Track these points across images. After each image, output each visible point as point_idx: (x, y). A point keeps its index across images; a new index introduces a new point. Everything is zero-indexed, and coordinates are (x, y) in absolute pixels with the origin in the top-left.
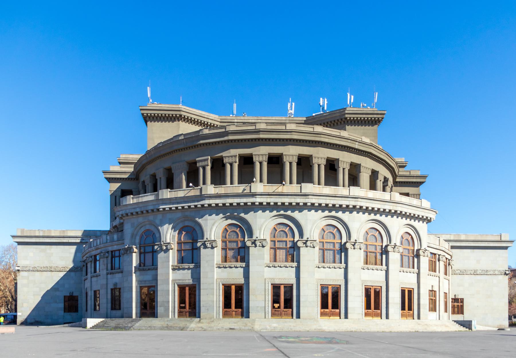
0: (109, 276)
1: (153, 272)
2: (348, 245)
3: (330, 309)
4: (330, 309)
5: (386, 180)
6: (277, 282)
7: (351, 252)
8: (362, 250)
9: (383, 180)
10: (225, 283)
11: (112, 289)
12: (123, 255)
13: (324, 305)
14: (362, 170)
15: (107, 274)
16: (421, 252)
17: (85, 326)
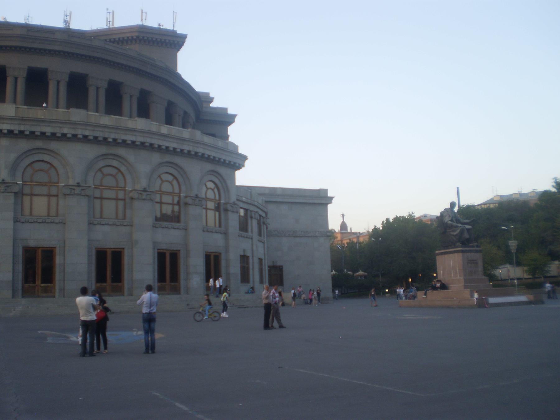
3: (109, 283)
4: (109, 283)
6: (32, 244)
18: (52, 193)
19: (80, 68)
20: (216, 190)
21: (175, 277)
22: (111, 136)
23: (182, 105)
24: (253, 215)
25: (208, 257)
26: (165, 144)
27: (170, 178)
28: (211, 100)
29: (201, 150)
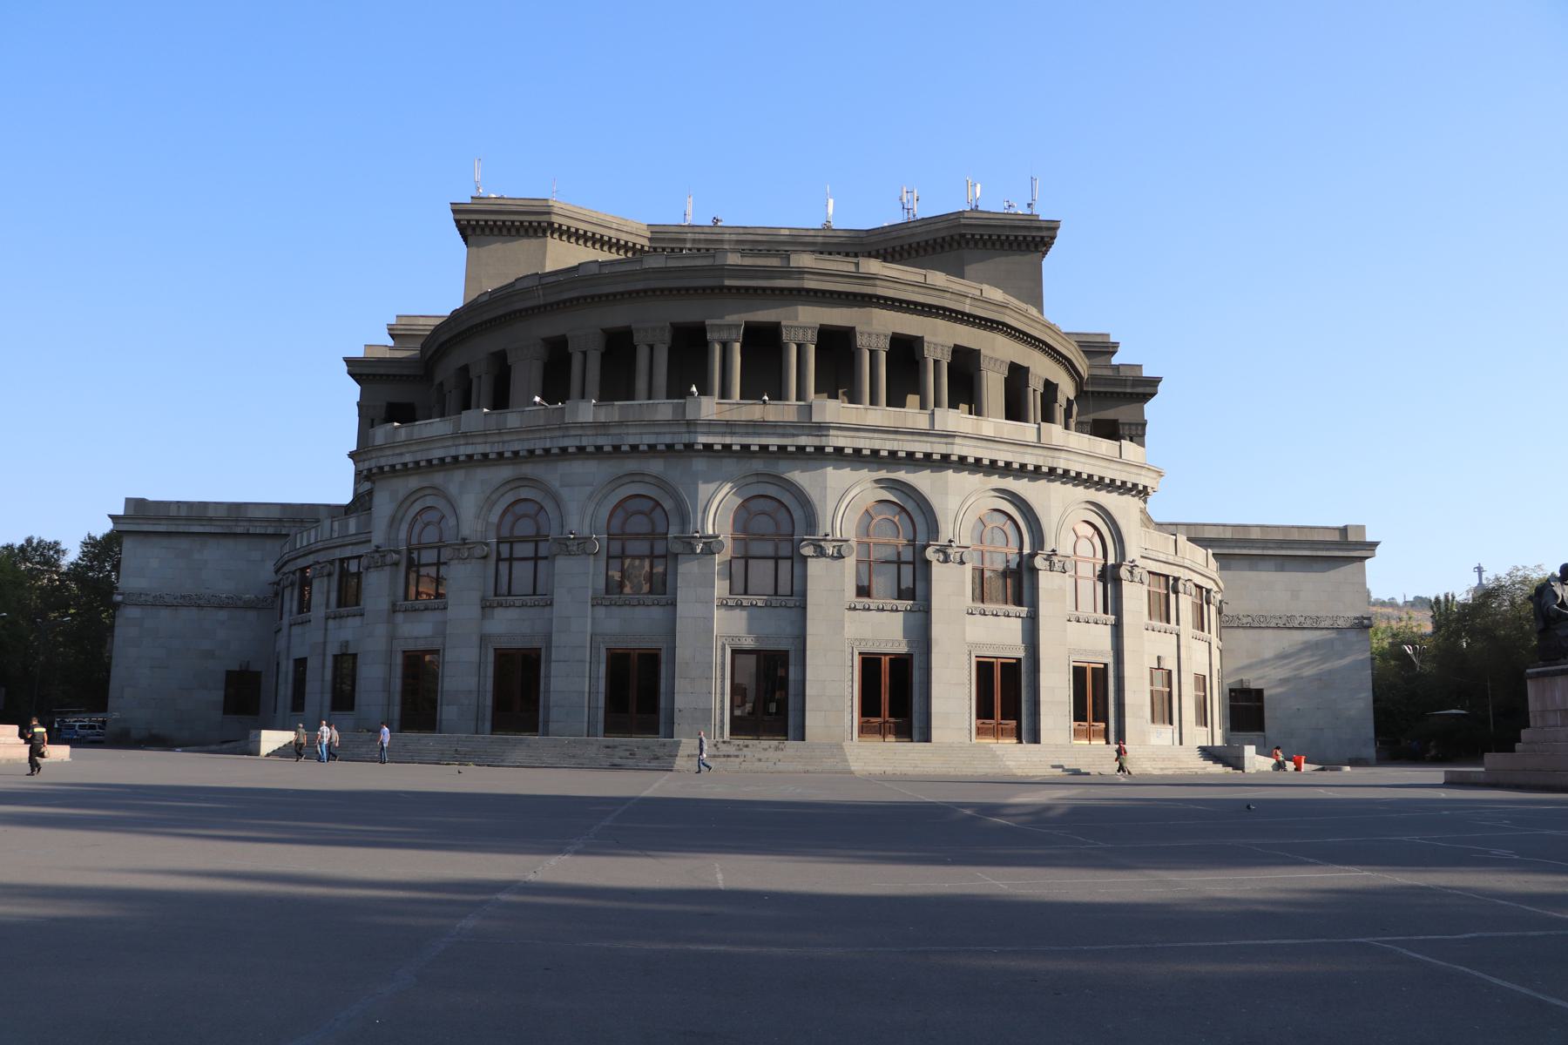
0: (331, 622)
1: (437, 615)
2: (930, 553)
5: (1050, 388)
7: (937, 569)
8: (968, 567)
9: (1041, 389)
10: (612, 646)
11: (335, 656)
12: (367, 568)
13: (869, 706)
14: (983, 366)
15: (327, 618)
16: (1124, 573)
17: (257, 753)
18: (781, 553)
19: (837, 317)
20: (1097, 540)
21: (1012, 710)
22: (885, 445)
23: (1042, 368)
24: (1181, 588)
25: (1079, 673)
26: (987, 454)
27: (1001, 519)
28: (1111, 349)
29: (1061, 464)
